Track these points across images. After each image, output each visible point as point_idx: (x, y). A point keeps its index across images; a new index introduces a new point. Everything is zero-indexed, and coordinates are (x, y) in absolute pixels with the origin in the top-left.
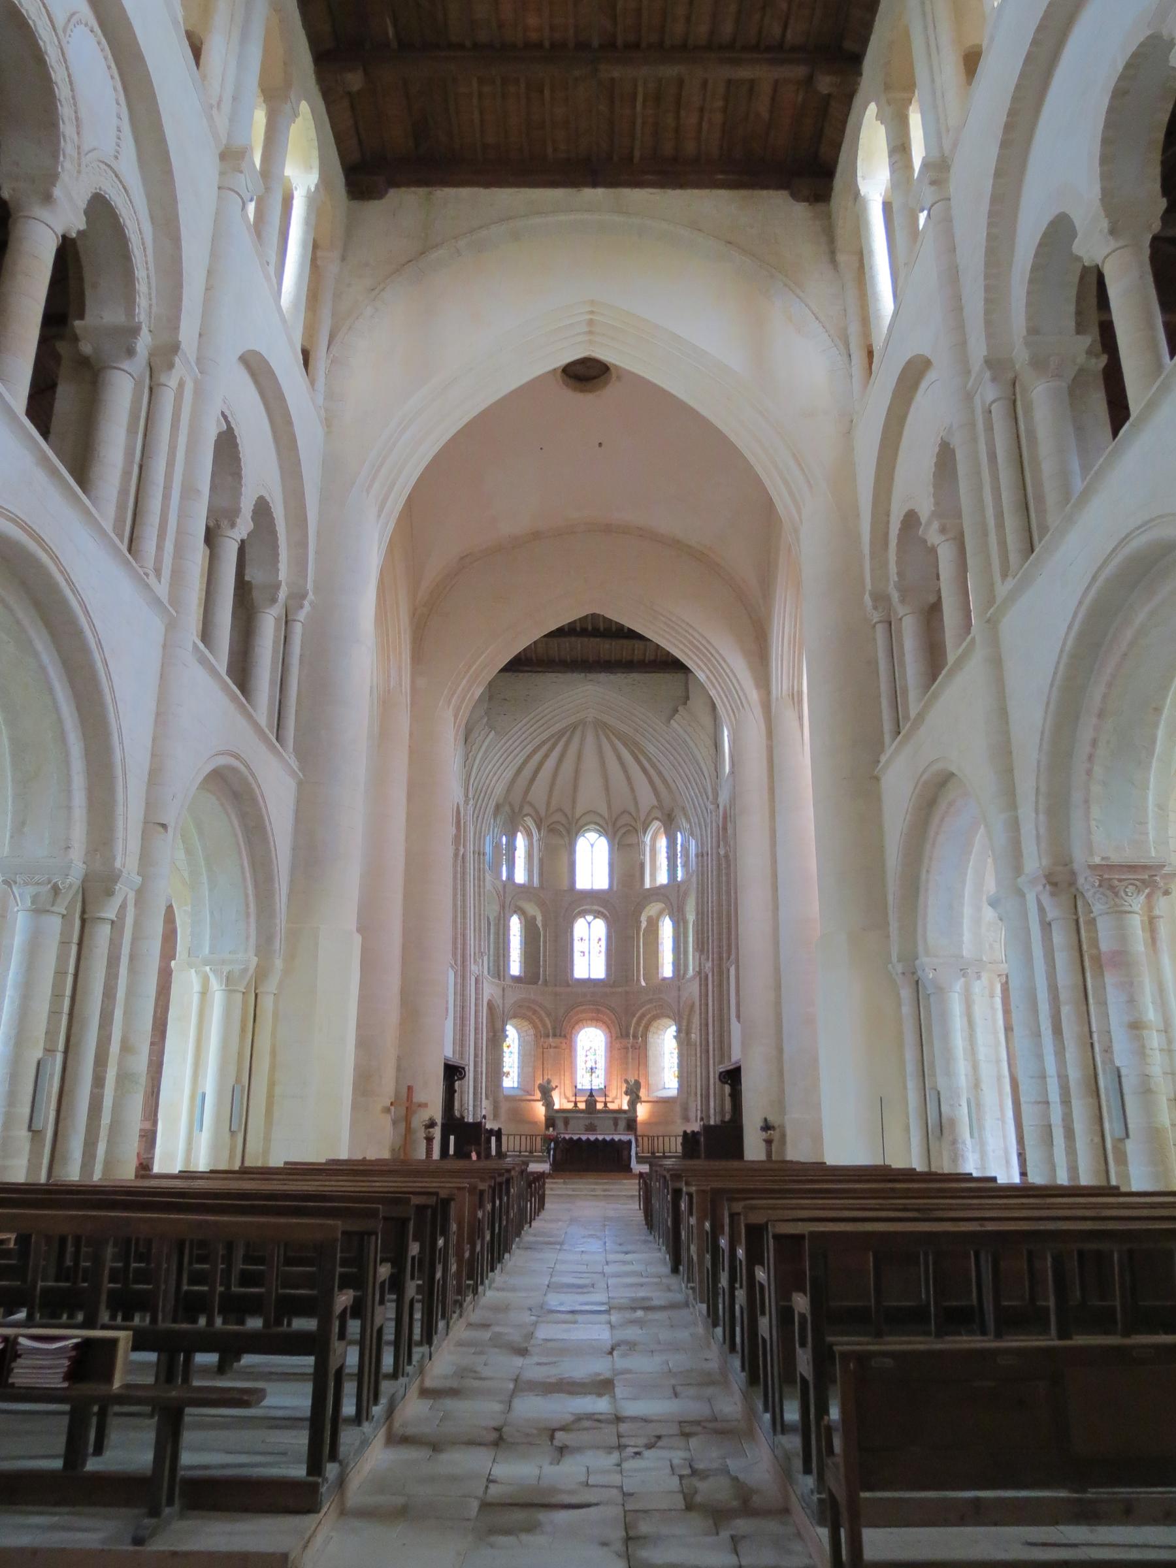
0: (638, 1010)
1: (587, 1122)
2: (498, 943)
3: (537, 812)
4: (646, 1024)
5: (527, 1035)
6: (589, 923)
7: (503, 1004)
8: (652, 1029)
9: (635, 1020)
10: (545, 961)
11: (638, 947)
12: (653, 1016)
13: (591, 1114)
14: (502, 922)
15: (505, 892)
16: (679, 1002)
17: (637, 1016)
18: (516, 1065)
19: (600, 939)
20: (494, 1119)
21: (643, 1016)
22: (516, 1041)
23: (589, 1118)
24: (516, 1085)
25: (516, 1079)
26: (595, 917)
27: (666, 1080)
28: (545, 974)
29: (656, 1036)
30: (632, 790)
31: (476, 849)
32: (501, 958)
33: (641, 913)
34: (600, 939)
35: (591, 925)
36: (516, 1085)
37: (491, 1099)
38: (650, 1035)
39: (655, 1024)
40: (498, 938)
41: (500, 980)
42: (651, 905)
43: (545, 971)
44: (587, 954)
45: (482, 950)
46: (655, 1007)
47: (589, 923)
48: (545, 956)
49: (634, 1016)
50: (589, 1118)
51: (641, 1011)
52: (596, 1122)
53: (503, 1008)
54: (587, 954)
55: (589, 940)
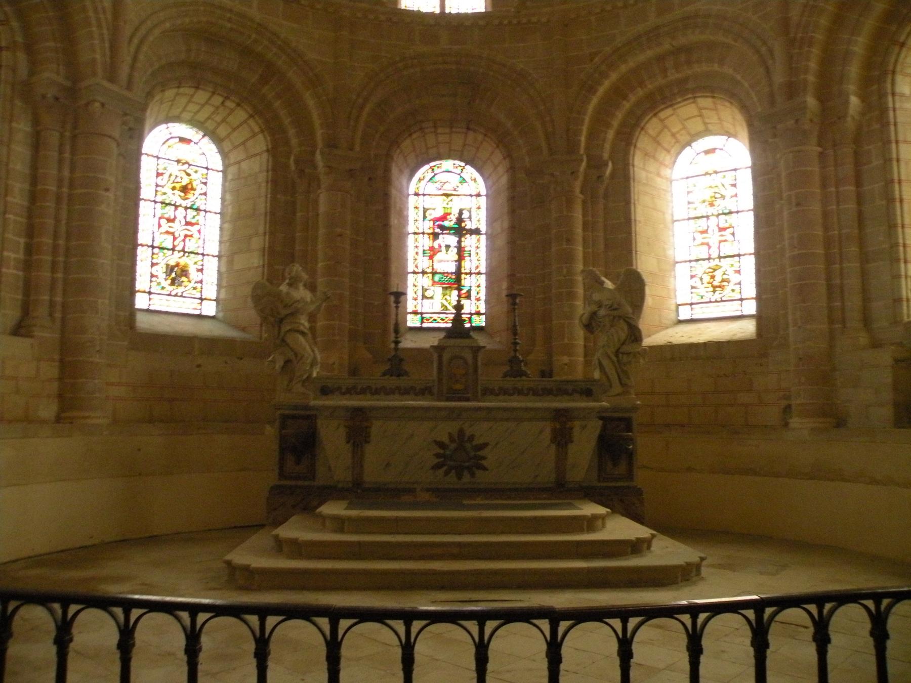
0: (604, 75)
1: (444, 431)
4: (623, 124)
5: (249, 157)
8: (643, 142)
9: (595, 101)
12: (650, 96)
13: (453, 395)
17: (601, 91)
18: (213, 246)
20: (58, 419)
21: (618, 93)
22: (216, 181)
23: (453, 415)
24: (210, 309)
25: (211, 291)
27: (683, 295)
29: (652, 166)
36: (210, 309)
37: (47, 333)
38: (638, 160)
39: (653, 126)
46: (661, 58)
49: (592, 90)
50: (453, 415)
51: (614, 76)
52: (481, 431)
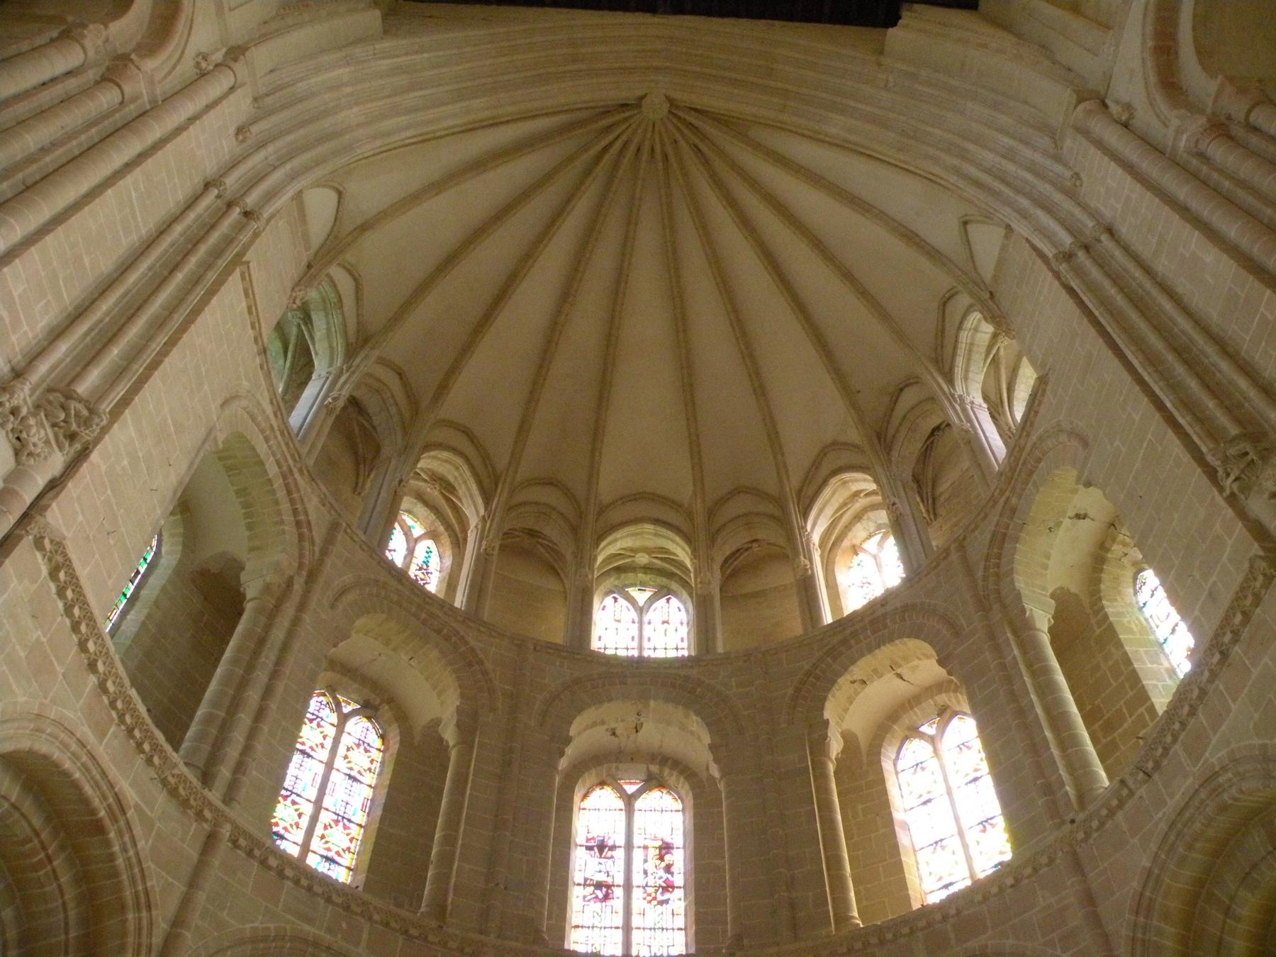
2: (250, 668)
3: (486, 458)
6: (629, 800)
7: (186, 902)
10: (449, 840)
11: (826, 806)
14: (289, 610)
15: (329, 540)
16: (1095, 919)
19: (666, 848)
26: (653, 782)
28: (441, 892)
30: (760, 391)
31: (231, 181)
32: (244, 719)
33: (825, 699)
34: (666, 848)
35: (639, 804)
40: (256, 654)
41: (207, 778)
42: (857, 671)
43: (443, 878)
44: (618, 892)
45: (82, 388)
47: (629, 800)
48: (452, 824)
53: (178, 922)
54: (618, 892)
55: (629, 847)
